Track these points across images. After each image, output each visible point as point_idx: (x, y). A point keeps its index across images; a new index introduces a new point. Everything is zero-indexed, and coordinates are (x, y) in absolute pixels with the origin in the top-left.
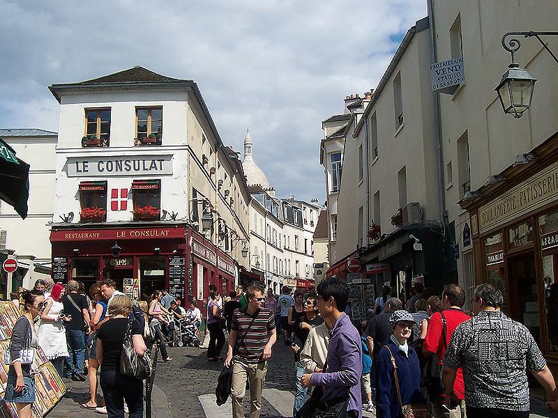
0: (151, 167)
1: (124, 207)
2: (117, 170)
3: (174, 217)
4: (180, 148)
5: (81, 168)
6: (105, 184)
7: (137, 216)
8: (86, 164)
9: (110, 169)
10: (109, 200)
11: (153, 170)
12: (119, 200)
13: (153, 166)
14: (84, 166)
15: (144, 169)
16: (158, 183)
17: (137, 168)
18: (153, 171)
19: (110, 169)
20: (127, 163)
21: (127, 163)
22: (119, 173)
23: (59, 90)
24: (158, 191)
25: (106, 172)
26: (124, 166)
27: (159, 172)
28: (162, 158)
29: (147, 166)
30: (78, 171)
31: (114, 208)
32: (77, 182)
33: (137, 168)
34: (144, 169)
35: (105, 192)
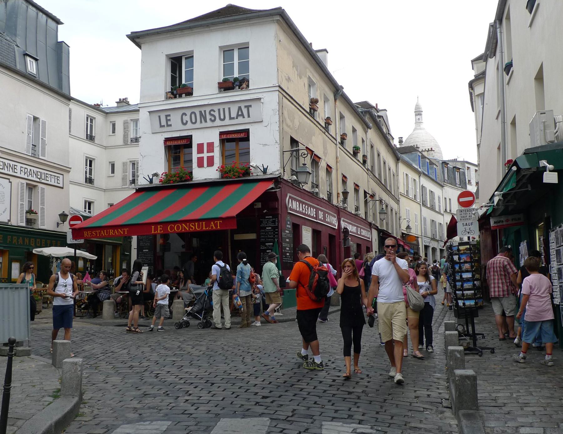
0: (238, 115)
1: (211, 162)
2: (201, 122)
3: (265, 171)
4: (268, 89)
5: (164, 122)
6: (190, 138)
7: (223, 171)
8: (168, 118)
9: (194, 120)
10: (195, 156)
11: (240, 118)
12: (205, 155)
13: (240, 114)
14: (167, 120)
15: (231, 118)
16: (247, 131)
17: (222, 117)
18: (240, 120)
19: (194, 120)
20: (212, 113)
21: (212, 113)
22: (204, 125)
23: (138, 37)
24: (247, 139)
25: (189, 125)
26: (208, 117)
27: (247, 120)
28: (248, 104)
29: (234, 114)
30: (161, 126)
31: (200, 164)
32: (160, 139)
33: (222, 117)
34: (231, 118)
35: (190, 146)
